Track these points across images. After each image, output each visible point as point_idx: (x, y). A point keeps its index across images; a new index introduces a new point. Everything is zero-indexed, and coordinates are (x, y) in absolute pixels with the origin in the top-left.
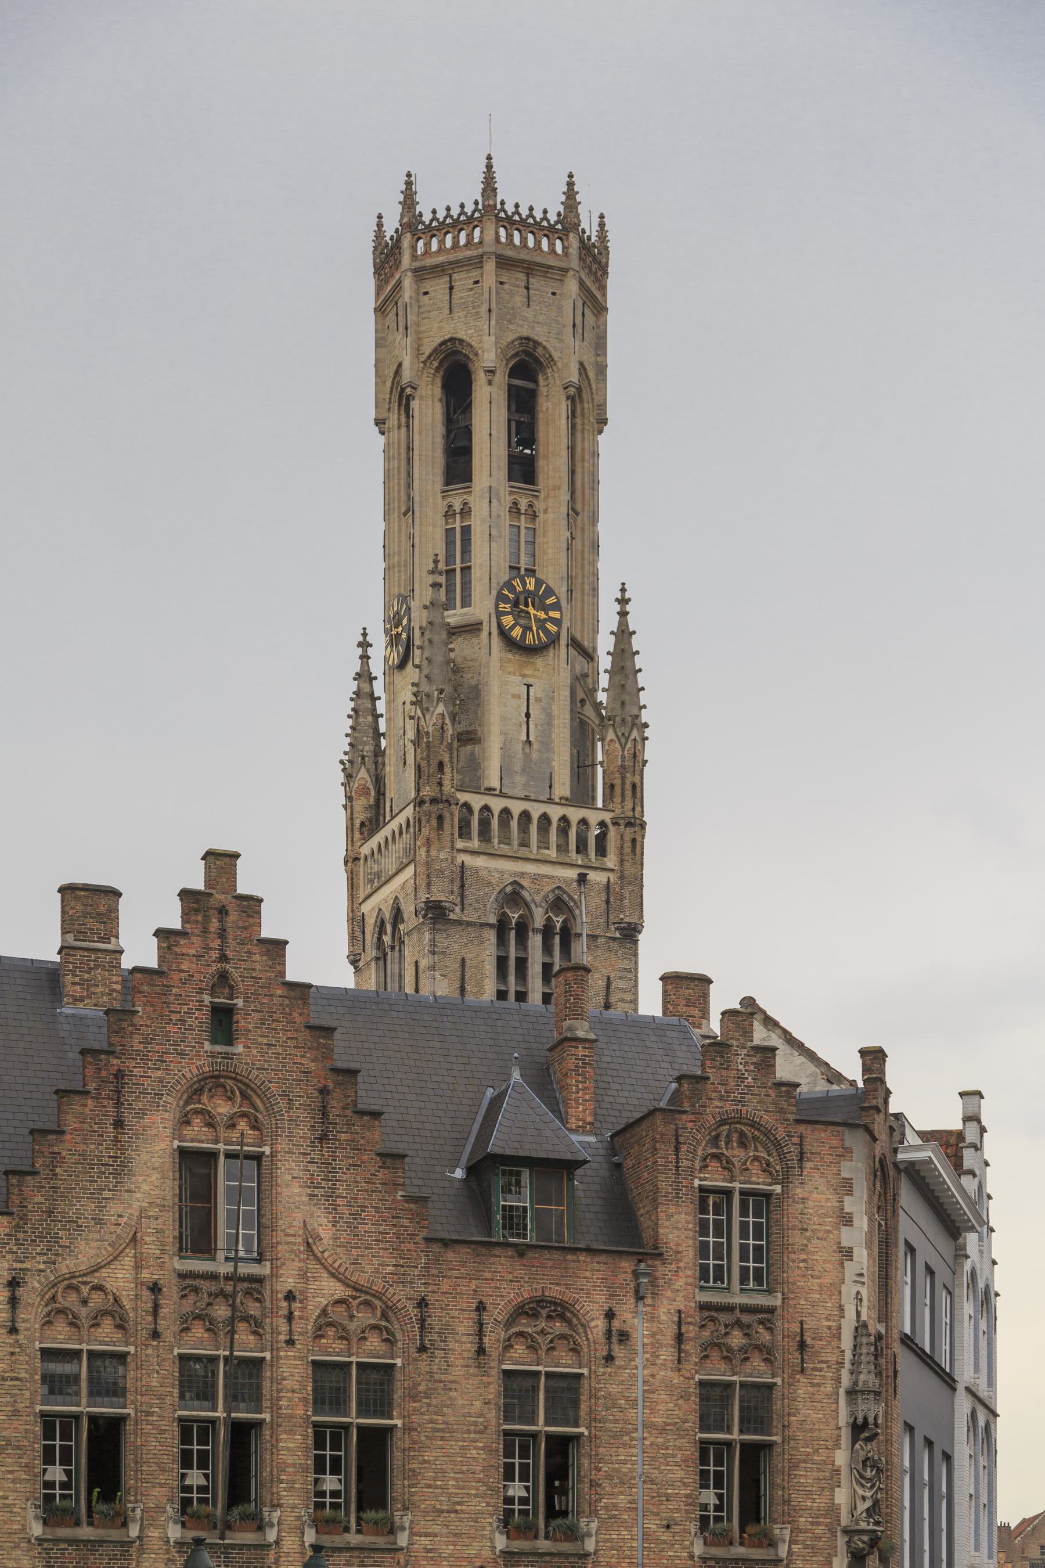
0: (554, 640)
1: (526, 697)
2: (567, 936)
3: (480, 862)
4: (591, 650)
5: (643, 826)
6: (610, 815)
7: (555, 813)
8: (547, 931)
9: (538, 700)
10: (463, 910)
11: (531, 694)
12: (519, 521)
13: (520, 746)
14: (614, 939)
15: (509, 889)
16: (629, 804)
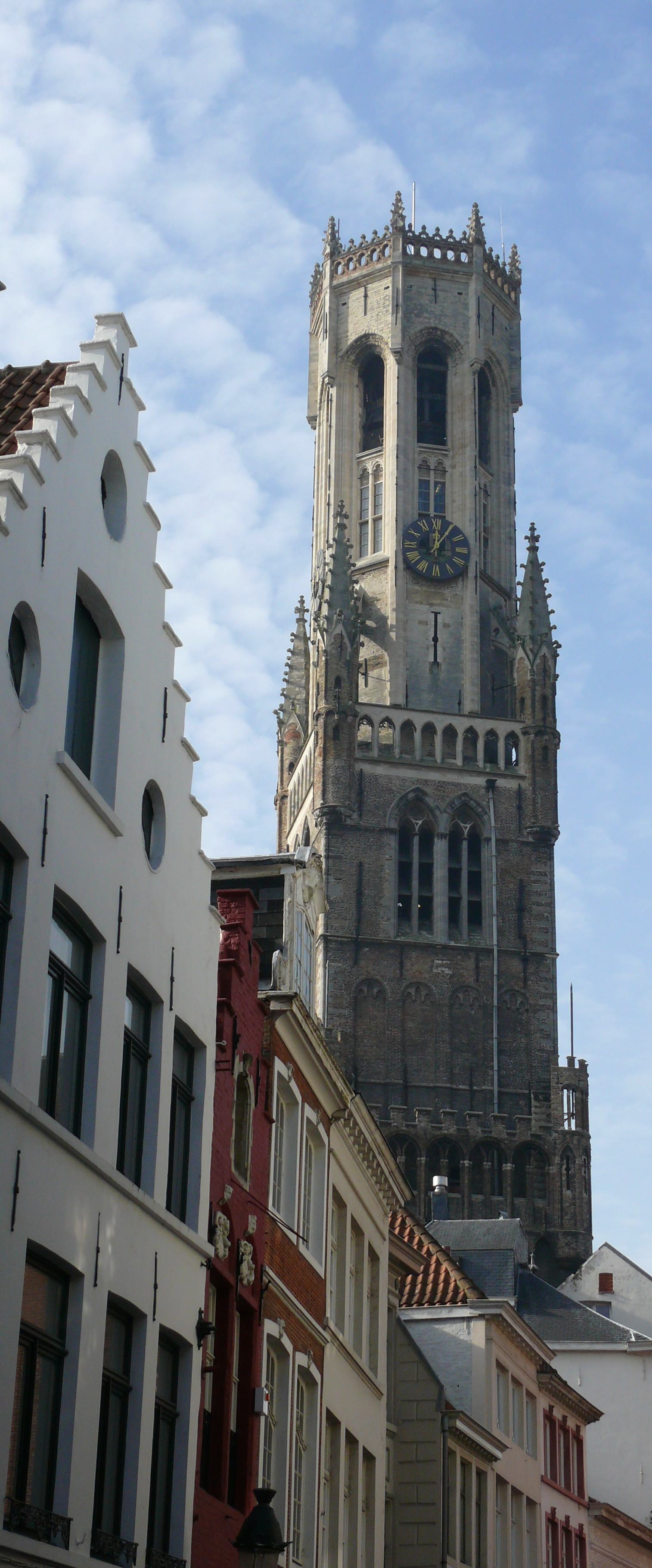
0: (462, 573)
2: (476, 842)
3: (380, 770)
4: (508, 590)
5: (556, 736)
6: (521, 726)
7: (461, 725)
9: (446, 626)
10: (360, 816)
11: (438, 620)
12: (429, 477)
13: (428, 667)
14: (527, 844)
16: (539, 715)
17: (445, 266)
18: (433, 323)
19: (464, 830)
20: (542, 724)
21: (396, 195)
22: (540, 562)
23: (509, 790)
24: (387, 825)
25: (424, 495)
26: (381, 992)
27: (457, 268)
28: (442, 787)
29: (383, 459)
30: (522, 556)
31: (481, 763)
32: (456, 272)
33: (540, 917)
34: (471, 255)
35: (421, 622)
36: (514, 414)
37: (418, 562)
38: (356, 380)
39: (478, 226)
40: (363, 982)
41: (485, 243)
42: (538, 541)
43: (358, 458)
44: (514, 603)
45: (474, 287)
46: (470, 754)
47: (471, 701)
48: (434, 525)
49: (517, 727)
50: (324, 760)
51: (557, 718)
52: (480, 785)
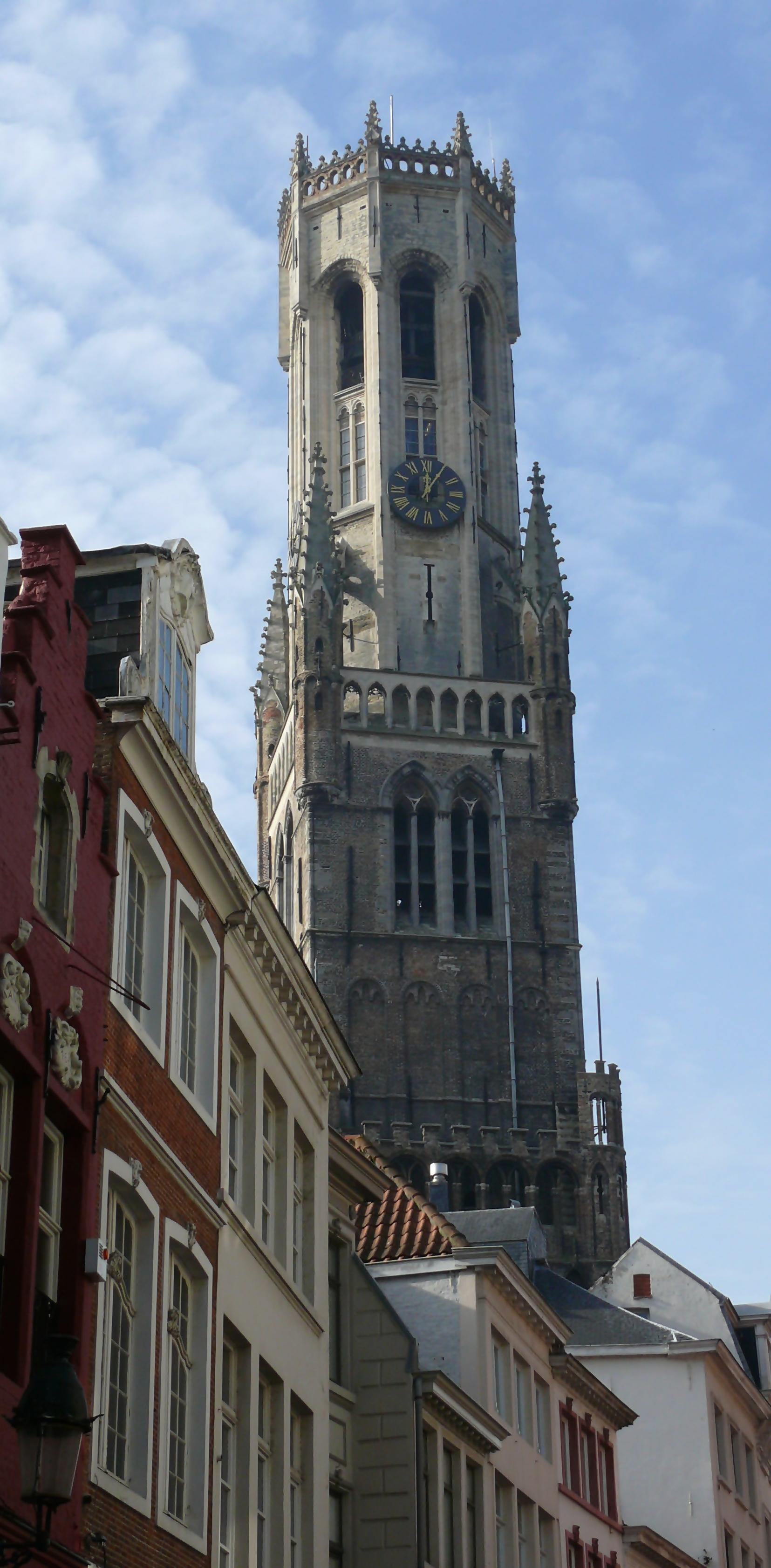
0: (457, 521)
1: (426, 577)
3: (370, 742)
4: (511, 539)
5: (571, 698)
6: (530, 688)
7: (461, 689)
8: (457, 818)
9: (441, 579)
10: (349, 795)
12: (417, 414)
14: (541, 821)
15: (407, 770)
16: (550, 676)
17: (428, 182)
18: (416, 244)
19: (468, 807)
20: (553, 685)
21: (371, 105)
22: (546, 505)
23: (518, 762)
24: (380, 805)
25: (412, 436)
26: (379, 994)
27: (441, 183)
28: (442, 760)
29: (365, 397)
30: (526, 499)
31: (485, 732)
32: (441, 188)
33: (559, 904)
34: (457, 169)
35: (412, 577)
36: (512, 345)
37: (407, 509)
38: (331, 311)
39: (464, 137)
40: (358, 982)
41: (473, 156)
42: (542, 482)
43: (337, 397)
44: (518, 554)
45: (461, 203)
46: (473, 722)
47: (472, 663)
48: (425, 468)
49: (525, 691)
50: (306, 732)
51: (571, 678)
52: (486, 757)
